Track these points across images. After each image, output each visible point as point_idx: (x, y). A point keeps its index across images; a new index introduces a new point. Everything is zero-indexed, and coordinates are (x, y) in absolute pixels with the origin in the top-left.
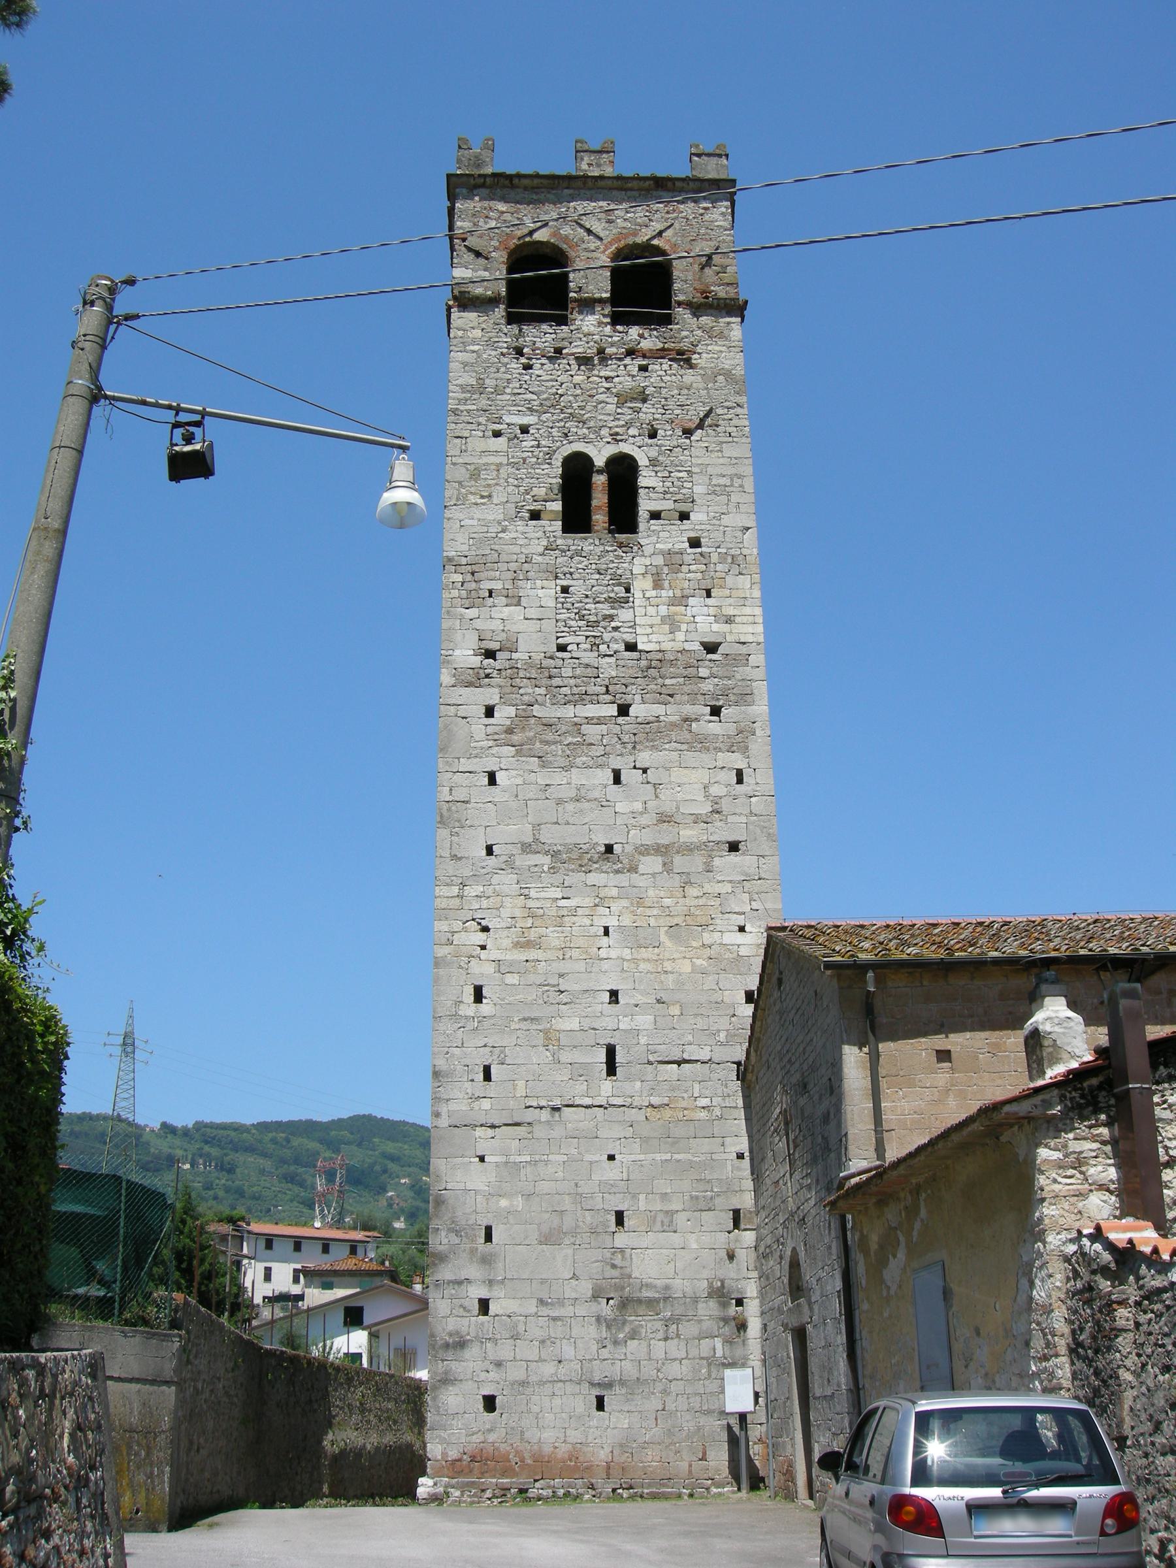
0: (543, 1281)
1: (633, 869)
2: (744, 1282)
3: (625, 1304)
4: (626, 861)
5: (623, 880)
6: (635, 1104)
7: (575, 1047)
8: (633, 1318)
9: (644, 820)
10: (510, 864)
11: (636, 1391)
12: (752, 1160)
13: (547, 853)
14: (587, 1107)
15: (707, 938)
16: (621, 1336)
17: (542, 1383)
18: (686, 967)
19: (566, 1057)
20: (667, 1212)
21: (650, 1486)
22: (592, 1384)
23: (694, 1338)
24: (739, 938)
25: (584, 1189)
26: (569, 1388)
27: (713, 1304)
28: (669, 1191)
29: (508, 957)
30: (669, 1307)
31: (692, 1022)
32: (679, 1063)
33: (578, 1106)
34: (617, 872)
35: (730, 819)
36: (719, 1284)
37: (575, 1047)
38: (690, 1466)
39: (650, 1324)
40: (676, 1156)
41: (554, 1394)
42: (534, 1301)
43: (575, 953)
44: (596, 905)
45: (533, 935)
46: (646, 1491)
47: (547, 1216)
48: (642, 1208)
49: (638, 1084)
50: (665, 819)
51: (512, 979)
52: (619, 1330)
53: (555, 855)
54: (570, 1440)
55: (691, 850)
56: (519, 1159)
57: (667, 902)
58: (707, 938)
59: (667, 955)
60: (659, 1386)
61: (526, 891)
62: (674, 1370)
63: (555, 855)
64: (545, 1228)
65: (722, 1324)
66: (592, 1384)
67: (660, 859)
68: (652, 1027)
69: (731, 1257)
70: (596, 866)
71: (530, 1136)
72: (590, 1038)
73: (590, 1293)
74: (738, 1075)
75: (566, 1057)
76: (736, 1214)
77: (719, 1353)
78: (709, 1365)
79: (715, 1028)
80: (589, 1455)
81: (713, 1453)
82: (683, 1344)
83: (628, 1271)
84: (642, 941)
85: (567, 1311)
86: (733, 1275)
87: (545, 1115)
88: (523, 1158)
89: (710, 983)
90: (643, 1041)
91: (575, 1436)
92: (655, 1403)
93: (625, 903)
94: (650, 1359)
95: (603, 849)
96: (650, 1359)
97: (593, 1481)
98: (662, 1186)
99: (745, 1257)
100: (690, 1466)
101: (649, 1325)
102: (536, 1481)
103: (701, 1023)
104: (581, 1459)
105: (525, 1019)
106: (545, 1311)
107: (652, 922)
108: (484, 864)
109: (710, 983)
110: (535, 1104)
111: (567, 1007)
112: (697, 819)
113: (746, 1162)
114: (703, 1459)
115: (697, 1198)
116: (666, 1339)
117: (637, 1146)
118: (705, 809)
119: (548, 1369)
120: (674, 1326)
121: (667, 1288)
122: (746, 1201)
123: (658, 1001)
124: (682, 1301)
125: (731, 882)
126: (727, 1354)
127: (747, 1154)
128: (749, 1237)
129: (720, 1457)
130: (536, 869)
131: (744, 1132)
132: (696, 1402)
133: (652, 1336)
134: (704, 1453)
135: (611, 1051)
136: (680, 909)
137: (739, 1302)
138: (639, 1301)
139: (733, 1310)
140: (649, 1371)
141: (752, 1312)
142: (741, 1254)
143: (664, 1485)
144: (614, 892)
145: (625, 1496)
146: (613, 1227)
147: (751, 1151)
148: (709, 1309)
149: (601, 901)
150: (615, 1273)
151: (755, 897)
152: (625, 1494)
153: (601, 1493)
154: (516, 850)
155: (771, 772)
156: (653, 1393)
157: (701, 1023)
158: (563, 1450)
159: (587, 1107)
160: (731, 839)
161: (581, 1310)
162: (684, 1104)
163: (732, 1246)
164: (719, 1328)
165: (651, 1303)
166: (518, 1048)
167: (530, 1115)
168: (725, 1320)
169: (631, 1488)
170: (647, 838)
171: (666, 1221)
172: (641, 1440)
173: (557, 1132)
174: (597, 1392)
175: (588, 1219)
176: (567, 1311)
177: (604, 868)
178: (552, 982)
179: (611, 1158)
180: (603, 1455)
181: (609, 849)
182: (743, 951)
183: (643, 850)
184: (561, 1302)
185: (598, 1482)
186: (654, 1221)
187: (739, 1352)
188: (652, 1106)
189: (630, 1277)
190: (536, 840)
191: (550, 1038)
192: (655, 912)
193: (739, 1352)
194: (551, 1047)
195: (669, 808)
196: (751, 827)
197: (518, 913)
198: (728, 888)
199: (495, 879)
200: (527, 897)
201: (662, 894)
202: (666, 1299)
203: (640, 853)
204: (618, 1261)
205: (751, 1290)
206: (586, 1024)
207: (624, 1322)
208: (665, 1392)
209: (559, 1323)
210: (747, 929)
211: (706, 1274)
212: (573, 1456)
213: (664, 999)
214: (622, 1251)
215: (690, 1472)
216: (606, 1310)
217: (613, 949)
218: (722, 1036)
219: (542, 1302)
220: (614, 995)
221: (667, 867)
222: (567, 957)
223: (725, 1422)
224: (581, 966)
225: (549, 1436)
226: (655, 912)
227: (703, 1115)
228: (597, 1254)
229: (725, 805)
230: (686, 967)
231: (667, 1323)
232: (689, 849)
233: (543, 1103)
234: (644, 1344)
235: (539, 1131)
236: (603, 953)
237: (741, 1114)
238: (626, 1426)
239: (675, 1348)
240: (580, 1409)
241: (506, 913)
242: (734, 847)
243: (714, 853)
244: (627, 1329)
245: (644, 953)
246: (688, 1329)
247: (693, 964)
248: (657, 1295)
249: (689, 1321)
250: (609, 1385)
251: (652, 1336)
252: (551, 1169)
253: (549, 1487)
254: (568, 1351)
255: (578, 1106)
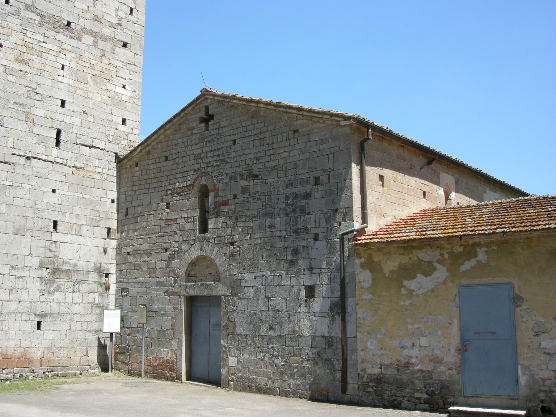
0: (14, 255)
1: (79, 39)
2: (109, 266)
3: (55, 271)
4: (76, 33)
5: (74, 42)
6: (68, 164)
7: (41, 126)
8: (58, 280)
9: (87, 16)
10: (17, 13)
11: (58, 320)
12: (118, 204)
13: (38, 14)
14: (44, 161)
15: (110, 86)
16: (52, 289)
17: (10, 314)
18: (98, 98)
19: (36, 130)
20: (78, 225)
21: (61, 370)
22: (36, 315)
23: (86, 293)
24: (120, 90)
25: (40, 206)
26: (24, 317)
27: (96, 275)
28: (80, 214)
29: (11, 65)
30: (76, 276)
31: (99, 127)
32: (91, 147)
33: (39, 159)
34: (72, 38)
35: (125, 30)
36: (99, 265)
37: (41, 126)
38: (81, 359)
39: (67, 284)
40: (85, 196)
41: (16, 320)
42: (8, 266)
43: (46, 74)
44: (59, 52)
45: (26, 57)
46: (60, 373)
47: (18, 218)
48: (67, 221)
49: (70, 154)
50: (96, 19)
51: (12, 78)
52: (51, 285)
53: (42, 17)
54: (22, 346)
55: (106, 39)
56: (6, 183)
57: (93, 62)
58: (110, 86)
59: (90, 90)
60: (69, 317)
61: (25, 32)
62: (76, 309)
63: (42, 17)
64: (17, 225)
65: (99, 286)
66: (36, 315)
67: (92, 39)
68: (80, 125)
69: (105, 252)
70: (62, 30)
71: (13, 171)
72: (49, 123)
73: (38, 265)
74: (115, 160)
75: (36, 130)
76: (109, 229)
77: (97, 301)
78: (92, 306)
79: (107, 133)
80: (32, 354)
81: (91, 352)
82: (81, 295)
83: (57, 254)
84: (79, 78)
85: (25, 273)
86: (105, 261)
87: (22, 160)
88: (8, 183)
89: (108, 109)
90: (75, 131)
91: (25, 344)
92: (66, 326)
93: (74, 55)
94: (65, 302)
95: (66, 23)
96: (65, 302)
97: (34, 368)
98: (77, 211)
99: (112, 253)
100: (81, 359)
101: (66, 284)
102: (3, 369)
103: (102, 129)
104: (28, 356)
105: (16, 103)
106: (14, 273)
107: (85, 69)
108: (4, 8)
109: (108, 109)
110: (17, 153)
111: (39, 102)
112: (111, 25)
113: (115, 205)
114: (86, 355)
115: (93, 219)
116: (73, 292)
117: (66, 187)
118: (115, 21)
119: (14, 306)
120: (78, 286)
121: (75, 265)
122: (114, 224)
123: (84, 112)
124: (82, 272)
125: (122, 62)
126: (100, 301)
127: (116, 201)
128: (114, 243)
129: (94, 354)
130: (31, 21)
131: (115, 189)
132: (85, 326)
133: (66, 290)
134: (87, 352)
135: (59, 132)
136: (98, 67)
137: (107, 275)
138: (62, 271)
139: (104, 279)
140: (64, 309)
141: (113, 279)
142: (110, 251)
143: (68, 369)
144: (69, 48)
145: (50, 376)
146: (52, 229)
147: (118, 199)
148: (94, 277)
149: (62, 51)
150: (51, 254)
151: (132, 73)
152: (50, 375)
153: (38, 375)
154: (22, 7)
155: (144, 15)
156: (65, 321)
157: (102, 129)
158: (19, 352)
159: (44, 161)
160: (124, 41)
161: (33, 273)
162: (90, 169)
163: (106, 247)
164: (98, 288)
165: (67, 272)
166: (11, 119)
167: (14, 159)
168: (101, 284)
169: (52, 371)
170: (88, 25)
171: (78, 229)
172: (58, 346)
173: (28, 172)
174: (38, 319)
175: (40, 223)
176: (25, 273)
177: (66, 33)
178: (33, 86)
179: (54, 191)
180: (39, 354)
181: (69, 24)
182: (124, 98)
183: (86, 31)
184: (23, 268)
185: (36, 369)
186: (72, 229)
187: (106, 301)
188: (76, 167)
189: (58, 257)
190: (33, 5)
191: (29, 118)
192: (87, 65)
193: (106, 301)
194: (29, 123)
195: (99, 14)
196: (133, 38)
197: (19, 42)
198: (120, 64)
199: (9, 19)
200: (25, 35)
201: (91, 57)
202: (75, 271)
203: (83, 32)
204: (53, 248)
205: (113, 269)
206: (49, 114)
207: (54, 282)
208: (71, 320)
209: (21, 280)
210: (126, 87)
211: (94, 259)
212: (24, 355)
213: (87, 112)
214: (55, 242)
215: (80, 362)
216: (45, 273)
217: (66, 77)
218: (111, 138)
219: (12, 267)
220: (63, 103)
221: (95, 43)
222: (42, 75)
223: (97, 336)
224: (48, 82)
225: (12, 344)
226: (87, 65)
227: (98, 176)
228: (43, 243)
229: (124, 22)
230: (98, 98)
231: (75, 283)
232: (105, 38)
233: (22, 154)
234: (63, 294)
235: (18, 169)
236: (60, 79)
237: (115, 180)
238: (51, 338)
239: (77, 297)
240: (29, 329)
241: (13, 40)
242: (125, 45)
243: (116, 45)
244: (55, 286)
245: (80, 85)
246: (84, 287)
247: (101, 98)
248: (70, 269)
249: (84, 283)
250: (45, 316)
251: (66, 290)
252: (23, 192)
253: (11, 373)
254: (24, 296)
255: (39, 159)
